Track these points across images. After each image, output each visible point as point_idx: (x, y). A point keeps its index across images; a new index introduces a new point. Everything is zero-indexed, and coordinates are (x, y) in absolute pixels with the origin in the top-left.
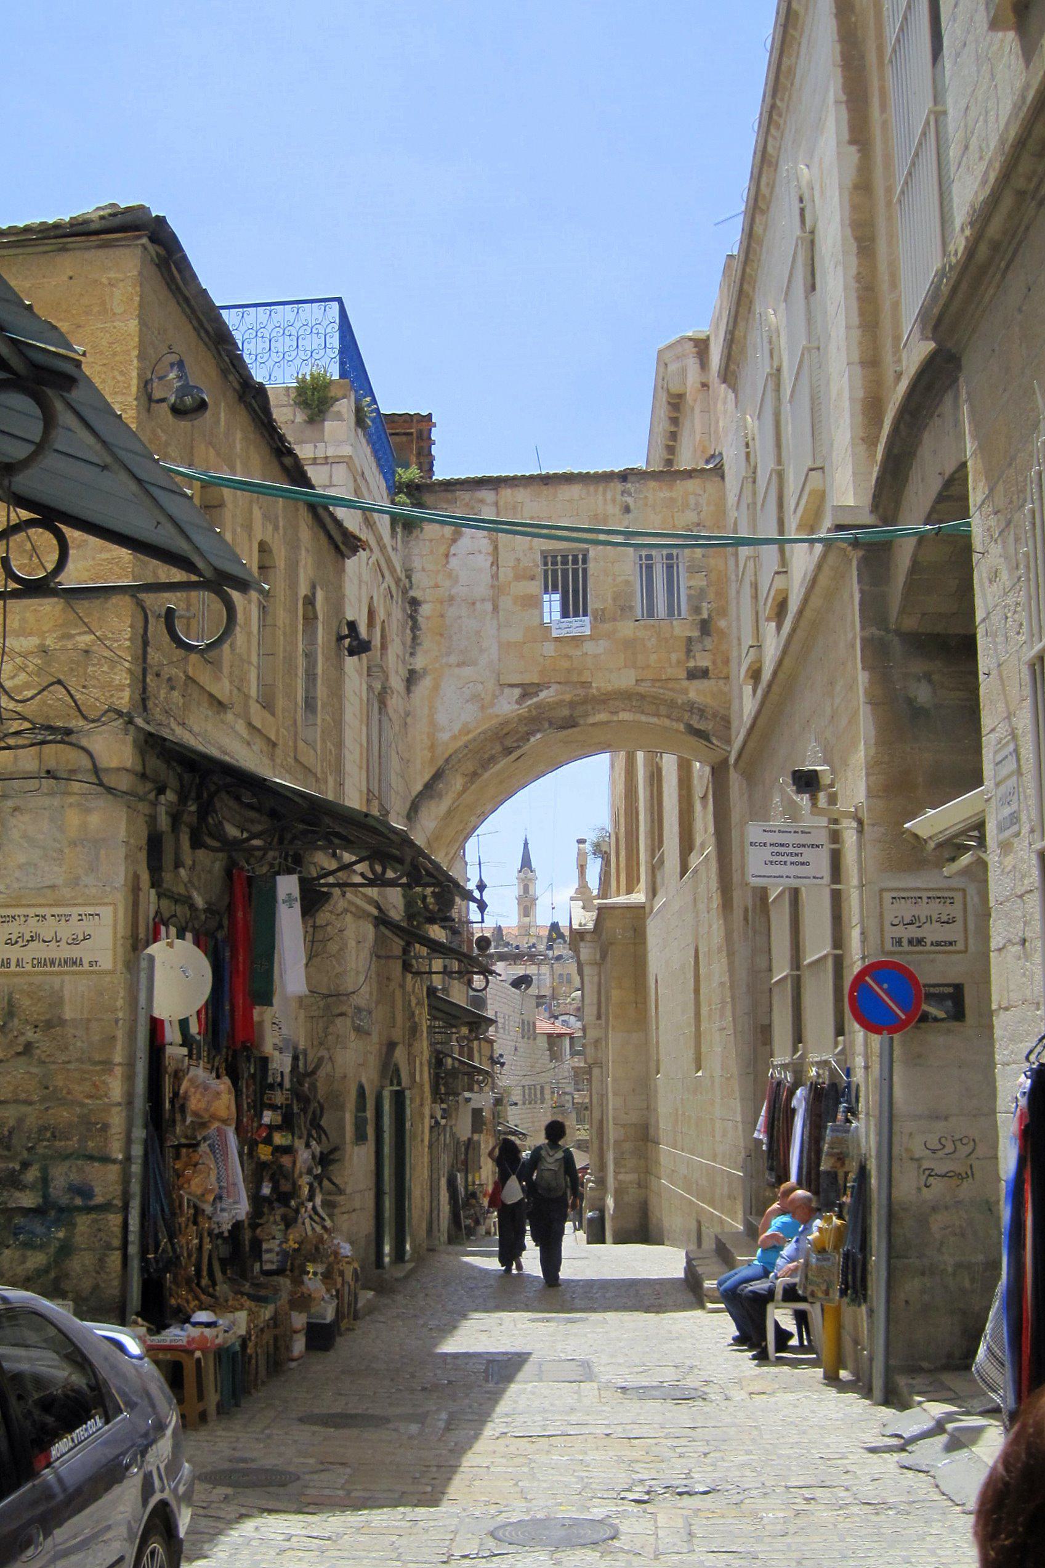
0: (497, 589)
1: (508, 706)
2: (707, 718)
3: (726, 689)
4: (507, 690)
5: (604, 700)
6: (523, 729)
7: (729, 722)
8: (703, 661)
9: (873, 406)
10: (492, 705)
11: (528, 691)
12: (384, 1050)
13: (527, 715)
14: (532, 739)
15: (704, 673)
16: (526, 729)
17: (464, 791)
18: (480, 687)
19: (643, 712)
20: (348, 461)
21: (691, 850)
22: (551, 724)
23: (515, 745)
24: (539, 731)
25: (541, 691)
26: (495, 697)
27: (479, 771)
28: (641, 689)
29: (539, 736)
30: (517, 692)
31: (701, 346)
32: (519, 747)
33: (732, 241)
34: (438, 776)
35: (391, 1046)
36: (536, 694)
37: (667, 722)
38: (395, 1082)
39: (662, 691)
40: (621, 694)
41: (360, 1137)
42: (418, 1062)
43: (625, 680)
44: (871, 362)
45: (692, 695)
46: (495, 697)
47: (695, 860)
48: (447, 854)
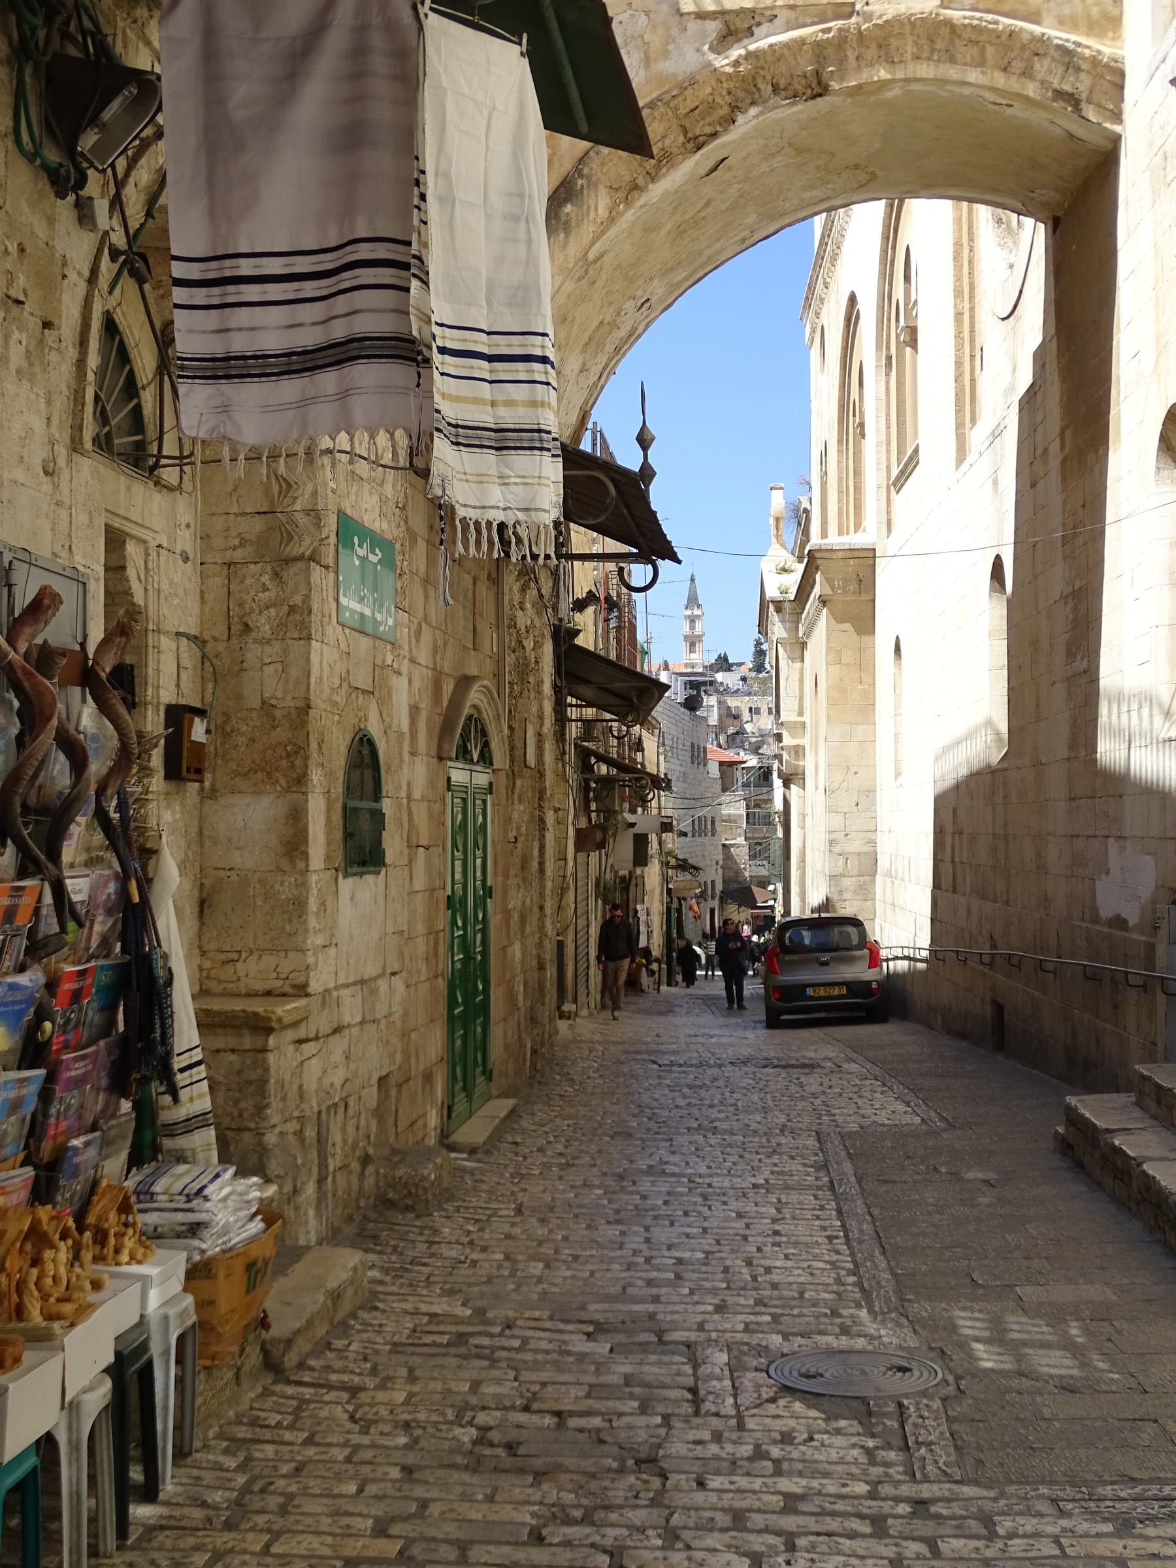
2: (1078, 69)
3: (1115, 12)
4: (693, 25)
6: (723, 100)
7: (1122, 75)
10: (666, 54)
12: (448, 687)
13: (729, 70)
14: (740, 119)
16: (728, 99)
17: (611, 220)
18: (643, 19)
19: (952, 60)
21: (974, 421)
22: (776, 89)
23: (708, 130)
24: (753, 103)
25: (759, 24)
26: (669, 39)
27: (640, 181)
29: (753, 111)
30: (713, 28)
32: (715, 135)
35: (465, 682)
36: (750, 32)
37: (1000, 80)
38: (476, 757)
39: (990, 17)
40: (913, 24)
41: (362, 852)
42: (530, 733)
46: (669, 39)
47: (977, 436)
48: (583, 370)
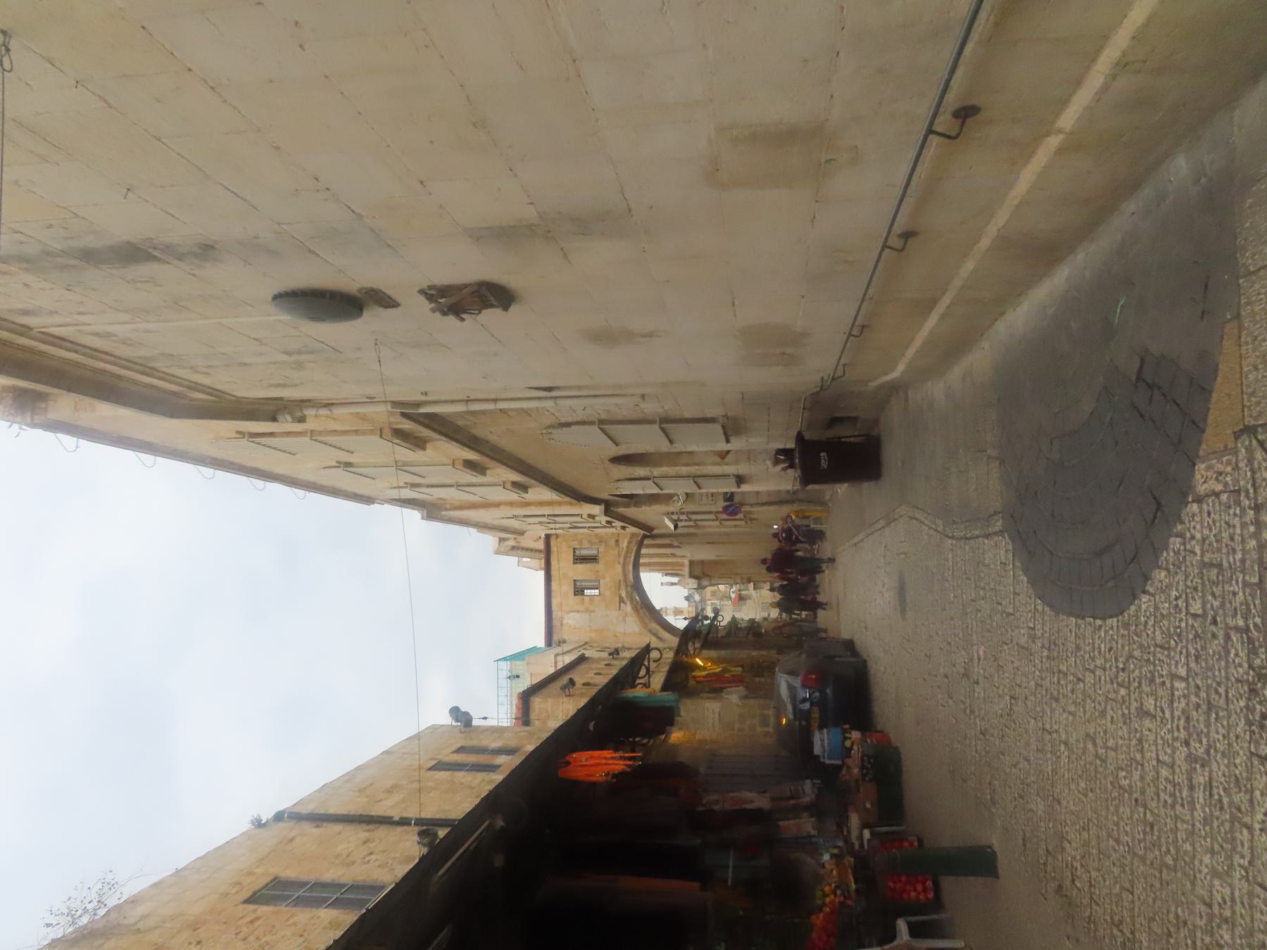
0: (587, 611)
1: (628, 608)
5: (625, 575)
8: (613, 542)
9: (571, 504)
11: (622, 600)
15: (617, 541)
20: (556, 655)
28: (622, 560)
31: (501, 540)
33: (473, 531)
34: (650, 631)
43: (619, 568)
44: (559, 504)
45: (625, 545)
47: (676, 544)
